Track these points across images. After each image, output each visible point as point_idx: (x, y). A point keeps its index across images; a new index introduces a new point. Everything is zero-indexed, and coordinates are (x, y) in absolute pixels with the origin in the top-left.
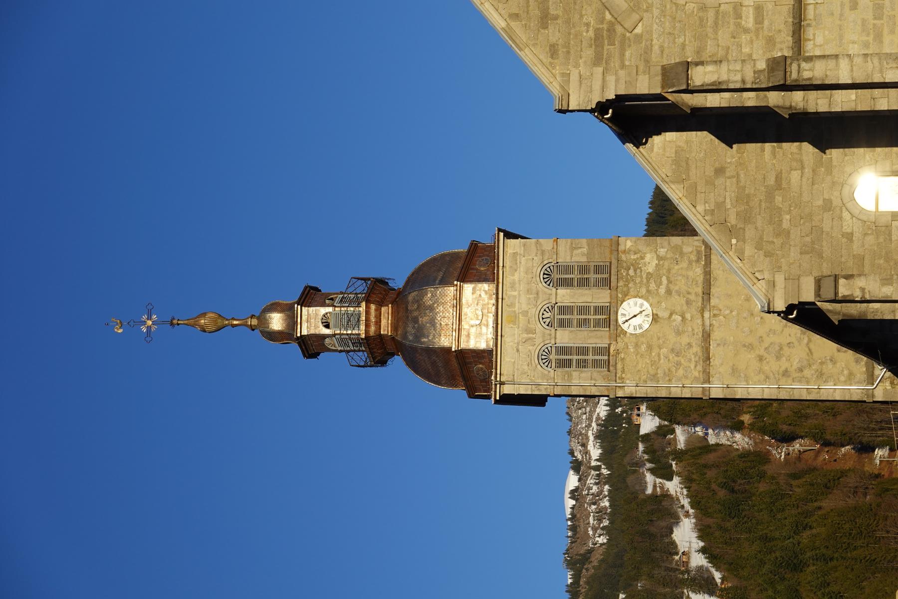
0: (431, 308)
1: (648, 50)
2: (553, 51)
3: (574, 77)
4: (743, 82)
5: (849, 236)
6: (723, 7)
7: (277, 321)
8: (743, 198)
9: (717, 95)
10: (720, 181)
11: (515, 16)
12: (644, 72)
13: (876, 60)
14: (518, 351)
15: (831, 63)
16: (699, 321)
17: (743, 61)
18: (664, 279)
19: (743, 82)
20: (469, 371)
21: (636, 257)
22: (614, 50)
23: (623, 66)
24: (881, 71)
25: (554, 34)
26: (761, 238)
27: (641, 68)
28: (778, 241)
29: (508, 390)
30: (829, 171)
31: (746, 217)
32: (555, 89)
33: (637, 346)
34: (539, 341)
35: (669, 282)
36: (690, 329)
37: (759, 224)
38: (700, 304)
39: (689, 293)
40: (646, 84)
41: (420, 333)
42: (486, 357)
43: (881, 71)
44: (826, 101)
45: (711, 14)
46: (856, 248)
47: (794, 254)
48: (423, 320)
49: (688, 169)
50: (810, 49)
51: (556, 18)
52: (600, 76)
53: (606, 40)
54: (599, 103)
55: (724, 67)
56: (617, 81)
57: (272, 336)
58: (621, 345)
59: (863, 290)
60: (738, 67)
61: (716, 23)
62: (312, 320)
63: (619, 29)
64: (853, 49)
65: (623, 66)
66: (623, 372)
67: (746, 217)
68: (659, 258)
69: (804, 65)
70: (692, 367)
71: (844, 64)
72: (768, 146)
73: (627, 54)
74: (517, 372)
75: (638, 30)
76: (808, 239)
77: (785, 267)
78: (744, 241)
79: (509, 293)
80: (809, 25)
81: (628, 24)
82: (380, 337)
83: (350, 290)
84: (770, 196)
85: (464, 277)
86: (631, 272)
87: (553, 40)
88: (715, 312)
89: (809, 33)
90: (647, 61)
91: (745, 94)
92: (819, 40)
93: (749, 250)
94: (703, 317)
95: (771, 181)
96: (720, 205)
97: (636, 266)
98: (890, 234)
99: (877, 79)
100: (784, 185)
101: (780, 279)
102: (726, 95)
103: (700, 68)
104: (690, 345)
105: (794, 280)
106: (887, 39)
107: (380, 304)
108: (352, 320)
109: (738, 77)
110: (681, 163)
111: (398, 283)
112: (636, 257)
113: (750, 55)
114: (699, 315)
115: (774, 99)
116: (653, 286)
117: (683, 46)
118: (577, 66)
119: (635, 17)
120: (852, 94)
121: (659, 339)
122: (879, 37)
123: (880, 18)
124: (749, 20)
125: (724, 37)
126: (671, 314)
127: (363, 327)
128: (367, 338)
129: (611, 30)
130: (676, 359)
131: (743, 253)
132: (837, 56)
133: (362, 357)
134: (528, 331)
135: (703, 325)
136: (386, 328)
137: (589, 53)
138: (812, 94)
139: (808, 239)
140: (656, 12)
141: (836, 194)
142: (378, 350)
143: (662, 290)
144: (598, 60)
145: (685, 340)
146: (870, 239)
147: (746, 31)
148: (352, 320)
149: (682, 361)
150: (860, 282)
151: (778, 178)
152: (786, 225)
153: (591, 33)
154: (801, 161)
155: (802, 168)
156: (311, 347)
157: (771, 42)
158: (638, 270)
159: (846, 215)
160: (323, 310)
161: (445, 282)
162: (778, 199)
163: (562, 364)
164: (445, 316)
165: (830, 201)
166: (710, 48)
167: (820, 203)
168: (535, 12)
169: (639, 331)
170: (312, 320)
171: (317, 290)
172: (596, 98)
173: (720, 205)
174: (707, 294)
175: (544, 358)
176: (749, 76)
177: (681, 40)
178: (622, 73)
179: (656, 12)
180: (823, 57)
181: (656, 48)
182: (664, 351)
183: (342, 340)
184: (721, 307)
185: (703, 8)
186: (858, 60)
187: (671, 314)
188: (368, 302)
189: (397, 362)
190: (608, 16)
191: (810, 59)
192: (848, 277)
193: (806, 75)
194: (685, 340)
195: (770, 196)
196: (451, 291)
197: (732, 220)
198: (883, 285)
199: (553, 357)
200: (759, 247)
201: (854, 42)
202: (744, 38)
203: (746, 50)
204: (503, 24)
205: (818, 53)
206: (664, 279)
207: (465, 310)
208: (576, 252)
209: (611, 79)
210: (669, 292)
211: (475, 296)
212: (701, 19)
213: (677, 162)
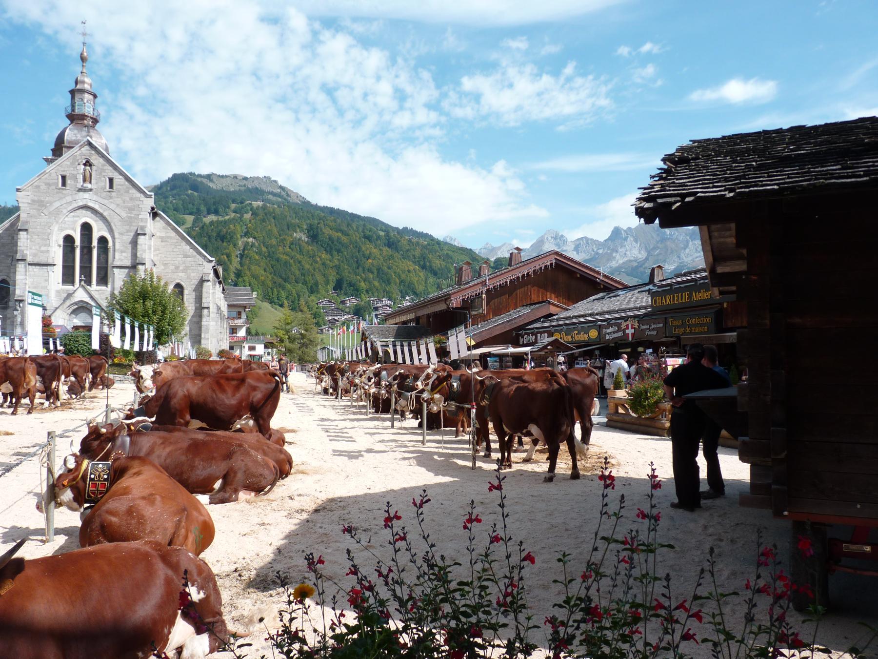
2: (38, 187)
22: (36, 206)
25: (43, 187)
71: (23, 277)
81: (45, 211)
124: (43, 248)
125: (37, 241)
129: (43, 206)
137: (36, 198)
144: (33, 201)
168: (51, 182)
209: (26, 205)
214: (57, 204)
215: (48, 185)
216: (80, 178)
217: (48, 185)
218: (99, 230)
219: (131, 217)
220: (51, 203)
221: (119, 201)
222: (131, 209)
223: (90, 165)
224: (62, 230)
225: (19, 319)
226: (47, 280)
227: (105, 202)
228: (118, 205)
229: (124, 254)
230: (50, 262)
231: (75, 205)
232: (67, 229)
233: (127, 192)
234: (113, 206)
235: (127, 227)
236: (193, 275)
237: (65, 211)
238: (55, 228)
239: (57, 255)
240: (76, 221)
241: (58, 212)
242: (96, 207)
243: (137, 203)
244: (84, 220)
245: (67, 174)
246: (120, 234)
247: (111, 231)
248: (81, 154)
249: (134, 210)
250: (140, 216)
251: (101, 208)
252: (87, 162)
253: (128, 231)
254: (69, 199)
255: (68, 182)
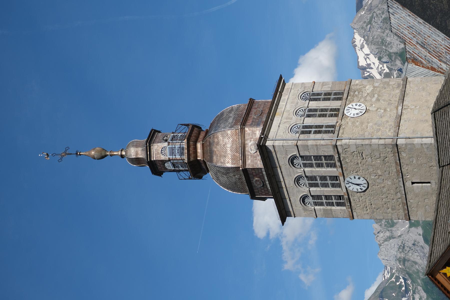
14: (279, 126)
16: (395, 112)
18: (376, 96)
21: (360, 87)
33: (353, 123)
35: (379, 95)
36: (389, 115)
38: (396, 105)
39: (390, 100)
58: (343, 122)
66: (343, 133)
68: (374, 87)
70: (387, 131)
83: (178, 131)
86: (356, 93)
88: (405, 107)
94: (397, 109)
97: (360, 91)
104: (387, 122)
112: (360, 87)
114: (396, 109)
116: (368, 98)
121: (368, 119)
126: (378, 109)
130: (378, 127)
135: (397, 113)
143: (374, 99)
145: (384, 119)
149: (381, 128)
158: (361, 93)
169: (356, 116)
174: (403, 99)
182: (371, 124)
184: (409, 105)
187: (378, 109)
194: (384, 119)
206: (376, 96)
208: (325, 86)
210: (378, 100)
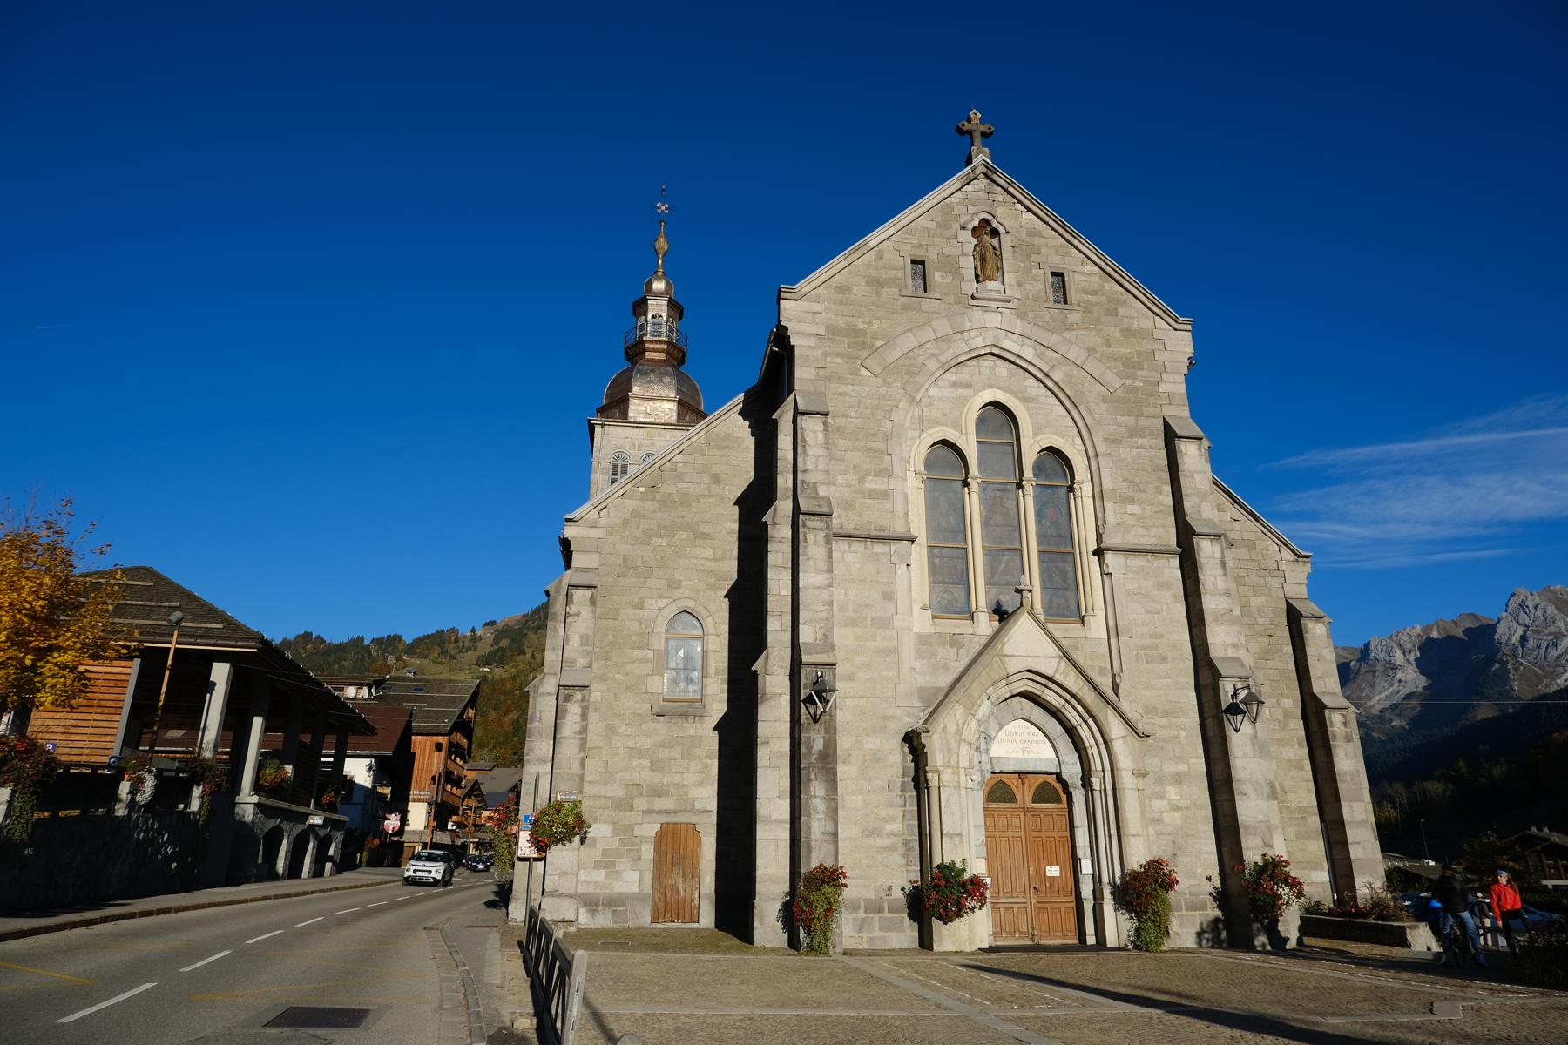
0: (660, 381)
1: (841, 379)
2: (843, 289)
3: (815, 307)
4: (805, 471)
5: (640, 606)
6: (887, 458)
7: (659, 286)
8: (686, 500)
9: (790, 447)
10: (706, 478)
11: (880, 256)
12: (818, 375)
13: (824, 615)
15: (823, 565)
17: (828, 472)
19: (805, 471)
20: (616, 407)
23: (825, 355)
24: (812, 621)
25: (861, 290)
26: (644, 517)
27: (822, 372)
28: (639, 533)
29: (598, 429)
30: (711, 587)
31: (666, 503)
32: (803, 286)
34: (633, 452)
37: (659, 515)
40: (805, 376)
41: (643, 373)
42: (624, 414)
43: (812, 621)
44: (780, 562)
45: (880, 446)
46: (627, 612)
47: (624, 548)
48: (652, 376)
49: (720, 448)
50: (840, 546)
51: (878, 294)
52: (815, 331)
53: (856, 342)
54: (786, 329)
55: (821, 452)
56: (810, 348)
57: (650, 284)
59: (578, 615)
60: (821, 466)
61: (870, 450)
62: (658, 308)
63: (865, 353)
64: (838, 595)
65: (825, 355)
67: (666, 503)
69: (822, 534)
71: (821, 579)
72: (736, 526)
73: (839, 360)
74: (611, 439)
75: (863, 372)
76: (639, 563)
77: (611, 539)
78: (642, 499)
79: (669, 433)
80: (866, 547)
81: (870, 362)
82: (644, 351)
84: (687, 527)
85: (681, 403)
87: (855, 290)
89: (858, 546)
90: (830, 379)
91: (790, 476)
92: (850, 557)
93: (631, 504)
95: (703, 529)
96: (680, 478)
98: (640, 648)
99: (803, 615)
100: (698, 541)
101: (599, 533)
102: (790, 457)
103: (821, 427)
105: (597, 547)
106: (849, 631)
107: (667, 352)
108: (656, 333)
109: (809, 466)
110: (727, 442)
111: (683, 369)
113: (834, 483)
115: (784, 506)
117: (847, 416)
118: (827, 310)
119: (878, 370)
120: (786, 591)
122: (852, 622)
123: (872, 625)
124: (872, 484)
125: (855, 457)
127: (648, 337)
128: (644, 342)
129: (864, 346)
131: (630, 498)
132: (830, 571)
133: (631, 342)
134: (640, 446)
136: (648, 355)
137: (841, 323)
138: (788, 548)
139: (639, 563)
140: (883, 390)
141: (687, 593)
142: (635, 351)
144: (833, 331)
146: (635, 627)
147: (861, 480)
148: (656, 333)
150: (586, 613)
151: (706, 536)
152: (656, 541)
153: (861, 326)
154: (722, 559)
155: (715, 560)
156: (640, 306)
157: (849, 505)
159: (663, 602)
160: (665, 315)
161: (679, 391)
162: (684, 535)
163: (615, 467)
164: (658, 390)
165: (679, 587)
166: (843, 443)
167: (677, 577)
168: (883, 275)
170: (658, 308)
171: (681, 317)
172: (792, 327)
173: (680, 478)
175: (620, 455)
176: (810, 478)
177: (853, 414)
178: (818, 353)
179: (883, 390)
180: (830, 552)
181: (844, 388)
183: (642, 327)
185: (887, 438)
186: (825, 595)
188: (669, 343)
189: (628, 365)
190: (879, 343)
191: (828, 542)
192: (593, 600)
193: (811, 537)
195: (687, 527)
196: (672, 394)
197: (664, 489)
198: (582, 637)
199: (620, 463)
200: (635, 514)
201: (846, 595)
202: (853, 479)
203: (840, 479)
204: (873, 244)
205: (835, 555)
207: (658, 404)
209: (812, 342)
211: (668, 410)
212: (874, 435)
213: (728, 437)
214: (908, 342)
215: (877, 283)
216: (968, 265)
217: (877, 283)
218: (1037, 431)
219: (1130, 390)
220: (889, 342)
221: (1094, 339)
222: (1130, 366)
223: (995, 233)
224: (922, 424)
225: (819, 745)
226: (889, 596)
227: (1054, 339)
228: (1091, 351)
229: (1132, 508)
230: (899, 529)
231: (959, 348)
232: (935, 423)
233: (1115, 313)
234: (1076, 354)
235: (1131, 420)
236: (1256, 601)
237: (932, 365)
238: (904, 414)
239: (911, 503)
240: (966, 399)
241: (910, 371)
242: (1028, 353)
243: (1148, 346)
244: (988, 396)
245: (929, 255)
246: (1111, 440)
247: (1084, 432)
248: (966, 202)
249: (1140, 366)
250: (1163, 388)
251: (1040, 356)
252: (985, 222)
253: (1134, 432)
254: (942, 326)
255: (936, 277)
